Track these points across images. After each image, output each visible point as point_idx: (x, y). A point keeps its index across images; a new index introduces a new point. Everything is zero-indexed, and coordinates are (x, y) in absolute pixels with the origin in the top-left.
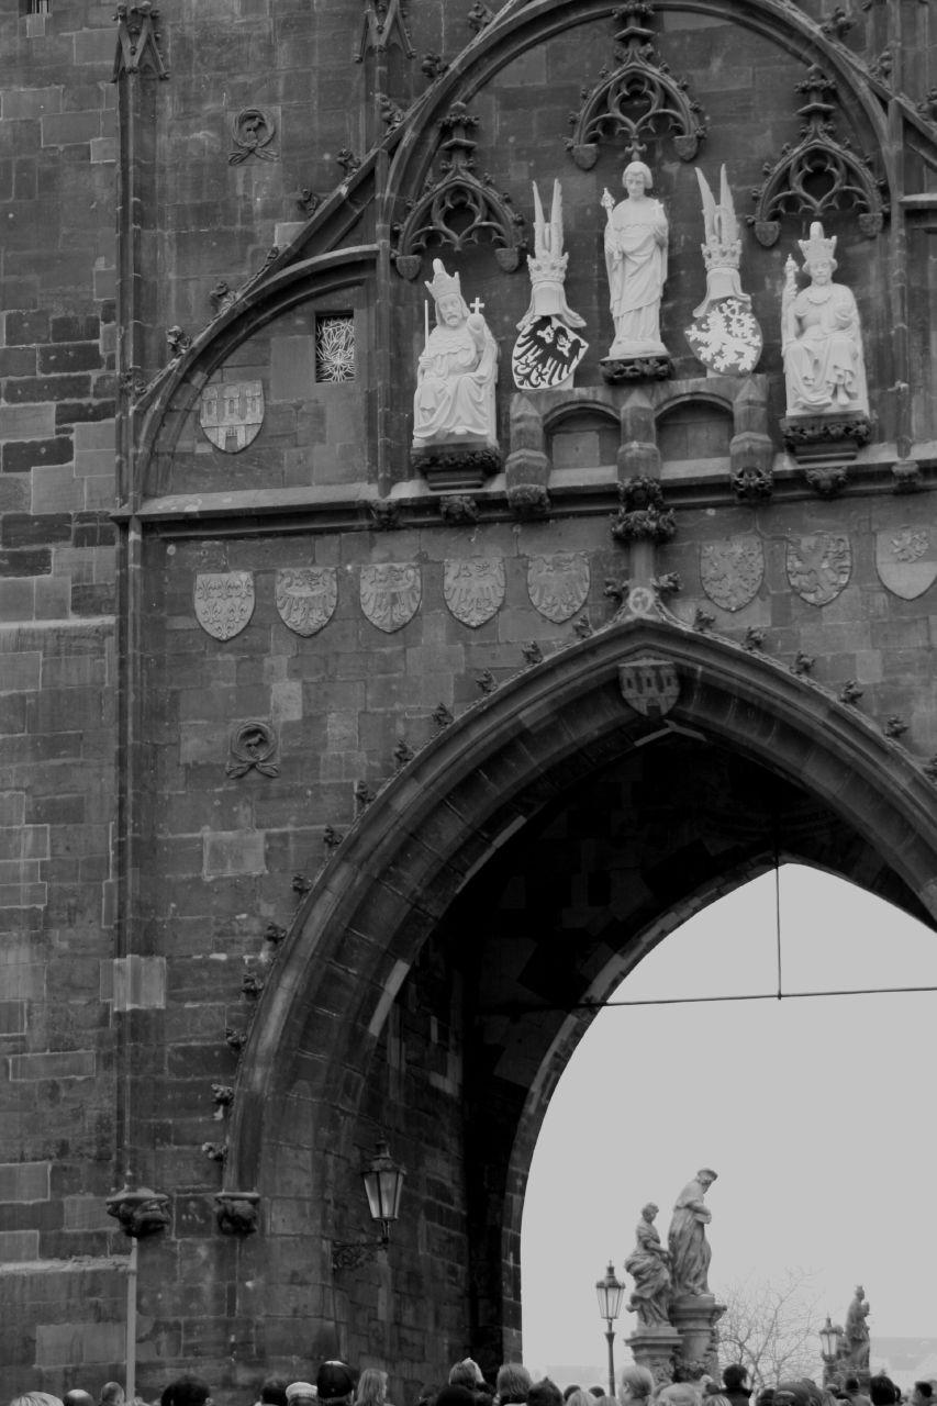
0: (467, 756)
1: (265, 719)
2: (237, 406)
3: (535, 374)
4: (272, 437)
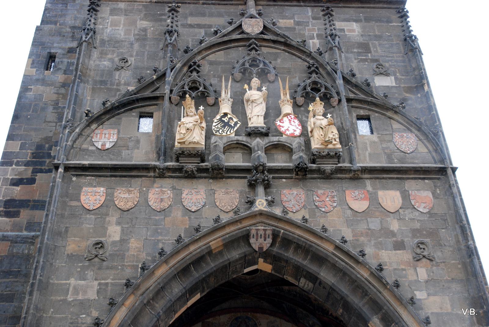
0: (188, 257)
1: (104, 239)
2: (107, 136)
3: (221, 131)
4: (119, 146)
